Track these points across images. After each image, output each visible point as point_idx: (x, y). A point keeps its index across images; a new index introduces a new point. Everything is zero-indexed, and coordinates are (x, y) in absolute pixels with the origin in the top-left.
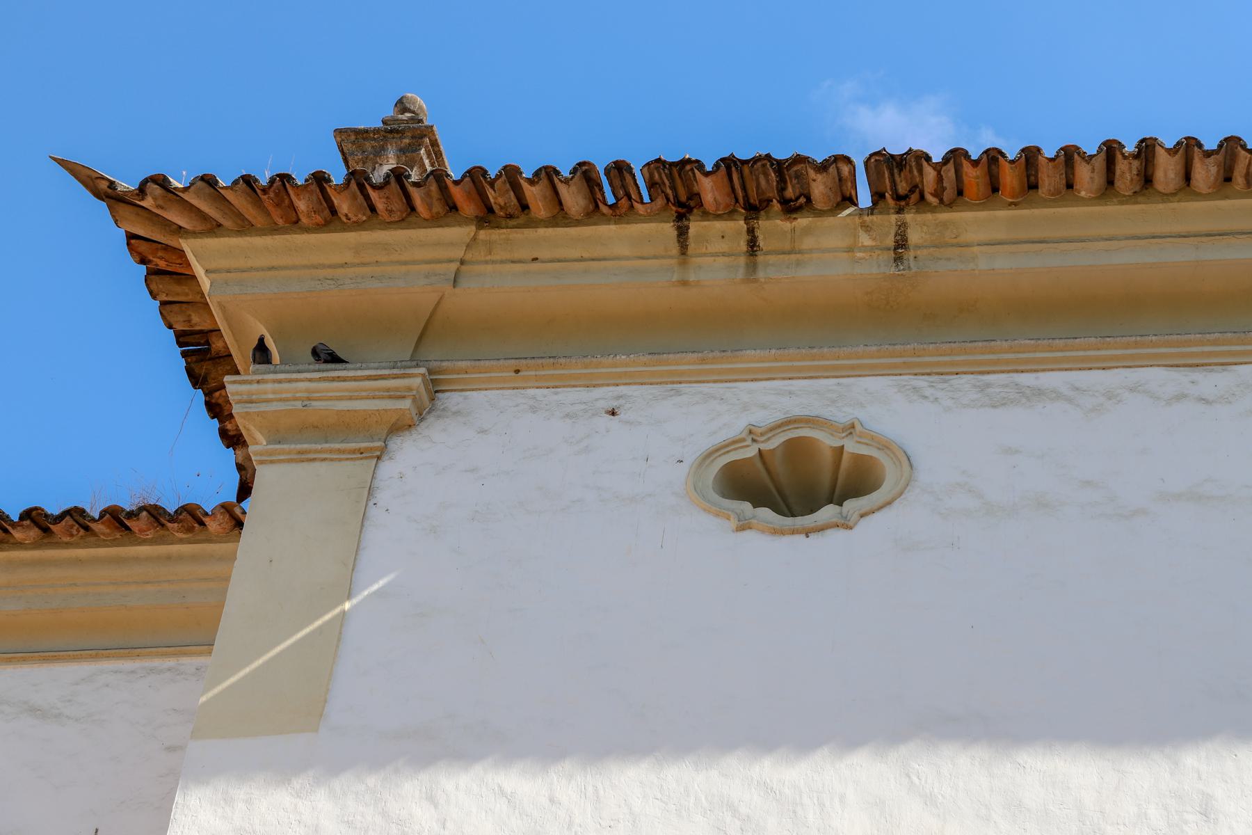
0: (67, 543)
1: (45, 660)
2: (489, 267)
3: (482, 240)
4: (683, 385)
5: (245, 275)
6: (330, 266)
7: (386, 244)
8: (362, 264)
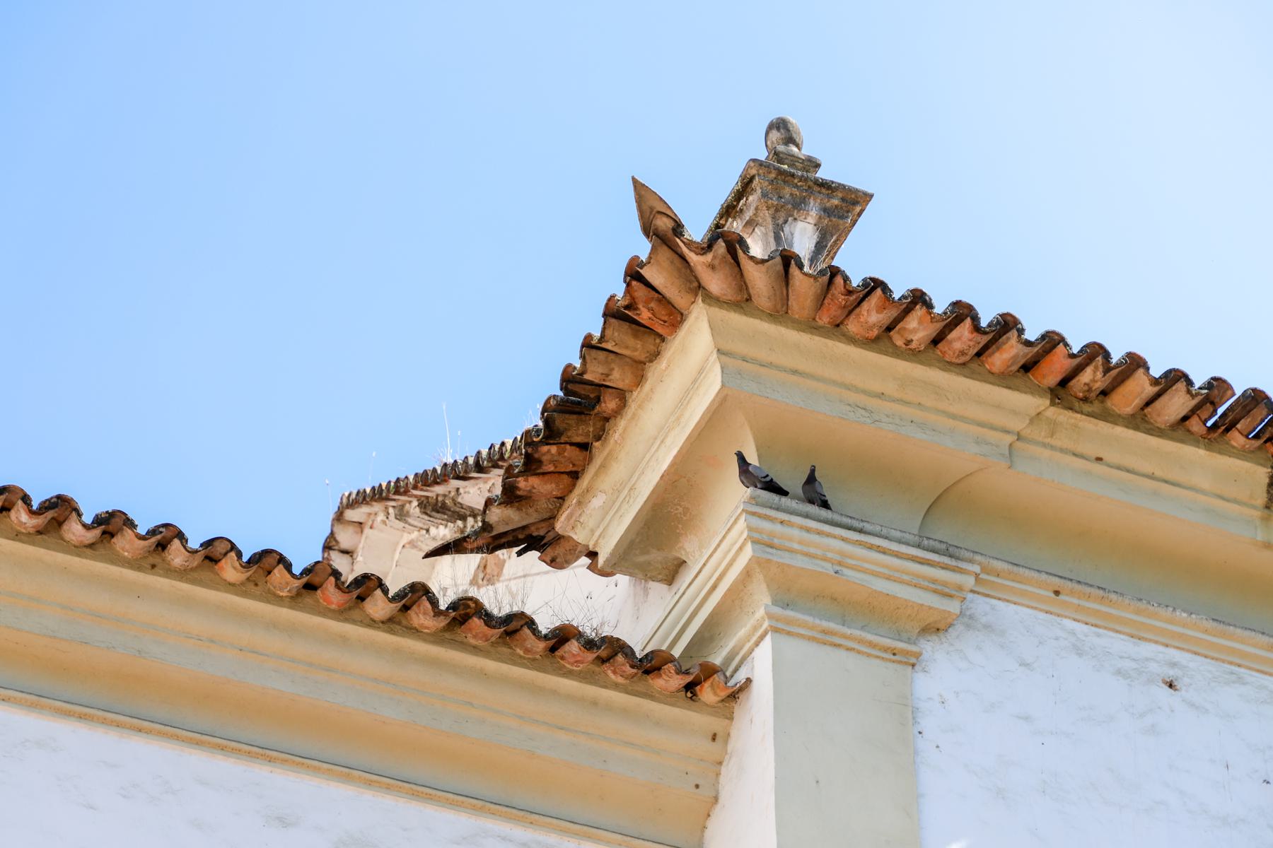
0: (475, 647)
1: (415, 796)
2: (1047, 453)
3: (1047, 418)
4: (1242, 670)
5: (763, 370)
6: (865, 392)
7: (939, 387)
8: (902, 401)
